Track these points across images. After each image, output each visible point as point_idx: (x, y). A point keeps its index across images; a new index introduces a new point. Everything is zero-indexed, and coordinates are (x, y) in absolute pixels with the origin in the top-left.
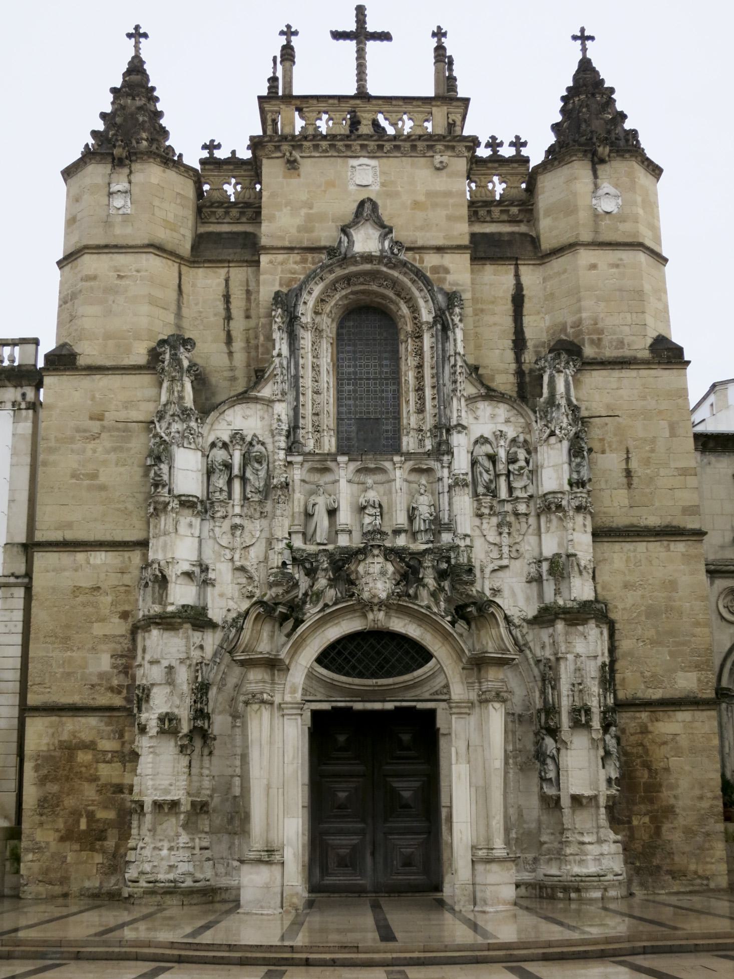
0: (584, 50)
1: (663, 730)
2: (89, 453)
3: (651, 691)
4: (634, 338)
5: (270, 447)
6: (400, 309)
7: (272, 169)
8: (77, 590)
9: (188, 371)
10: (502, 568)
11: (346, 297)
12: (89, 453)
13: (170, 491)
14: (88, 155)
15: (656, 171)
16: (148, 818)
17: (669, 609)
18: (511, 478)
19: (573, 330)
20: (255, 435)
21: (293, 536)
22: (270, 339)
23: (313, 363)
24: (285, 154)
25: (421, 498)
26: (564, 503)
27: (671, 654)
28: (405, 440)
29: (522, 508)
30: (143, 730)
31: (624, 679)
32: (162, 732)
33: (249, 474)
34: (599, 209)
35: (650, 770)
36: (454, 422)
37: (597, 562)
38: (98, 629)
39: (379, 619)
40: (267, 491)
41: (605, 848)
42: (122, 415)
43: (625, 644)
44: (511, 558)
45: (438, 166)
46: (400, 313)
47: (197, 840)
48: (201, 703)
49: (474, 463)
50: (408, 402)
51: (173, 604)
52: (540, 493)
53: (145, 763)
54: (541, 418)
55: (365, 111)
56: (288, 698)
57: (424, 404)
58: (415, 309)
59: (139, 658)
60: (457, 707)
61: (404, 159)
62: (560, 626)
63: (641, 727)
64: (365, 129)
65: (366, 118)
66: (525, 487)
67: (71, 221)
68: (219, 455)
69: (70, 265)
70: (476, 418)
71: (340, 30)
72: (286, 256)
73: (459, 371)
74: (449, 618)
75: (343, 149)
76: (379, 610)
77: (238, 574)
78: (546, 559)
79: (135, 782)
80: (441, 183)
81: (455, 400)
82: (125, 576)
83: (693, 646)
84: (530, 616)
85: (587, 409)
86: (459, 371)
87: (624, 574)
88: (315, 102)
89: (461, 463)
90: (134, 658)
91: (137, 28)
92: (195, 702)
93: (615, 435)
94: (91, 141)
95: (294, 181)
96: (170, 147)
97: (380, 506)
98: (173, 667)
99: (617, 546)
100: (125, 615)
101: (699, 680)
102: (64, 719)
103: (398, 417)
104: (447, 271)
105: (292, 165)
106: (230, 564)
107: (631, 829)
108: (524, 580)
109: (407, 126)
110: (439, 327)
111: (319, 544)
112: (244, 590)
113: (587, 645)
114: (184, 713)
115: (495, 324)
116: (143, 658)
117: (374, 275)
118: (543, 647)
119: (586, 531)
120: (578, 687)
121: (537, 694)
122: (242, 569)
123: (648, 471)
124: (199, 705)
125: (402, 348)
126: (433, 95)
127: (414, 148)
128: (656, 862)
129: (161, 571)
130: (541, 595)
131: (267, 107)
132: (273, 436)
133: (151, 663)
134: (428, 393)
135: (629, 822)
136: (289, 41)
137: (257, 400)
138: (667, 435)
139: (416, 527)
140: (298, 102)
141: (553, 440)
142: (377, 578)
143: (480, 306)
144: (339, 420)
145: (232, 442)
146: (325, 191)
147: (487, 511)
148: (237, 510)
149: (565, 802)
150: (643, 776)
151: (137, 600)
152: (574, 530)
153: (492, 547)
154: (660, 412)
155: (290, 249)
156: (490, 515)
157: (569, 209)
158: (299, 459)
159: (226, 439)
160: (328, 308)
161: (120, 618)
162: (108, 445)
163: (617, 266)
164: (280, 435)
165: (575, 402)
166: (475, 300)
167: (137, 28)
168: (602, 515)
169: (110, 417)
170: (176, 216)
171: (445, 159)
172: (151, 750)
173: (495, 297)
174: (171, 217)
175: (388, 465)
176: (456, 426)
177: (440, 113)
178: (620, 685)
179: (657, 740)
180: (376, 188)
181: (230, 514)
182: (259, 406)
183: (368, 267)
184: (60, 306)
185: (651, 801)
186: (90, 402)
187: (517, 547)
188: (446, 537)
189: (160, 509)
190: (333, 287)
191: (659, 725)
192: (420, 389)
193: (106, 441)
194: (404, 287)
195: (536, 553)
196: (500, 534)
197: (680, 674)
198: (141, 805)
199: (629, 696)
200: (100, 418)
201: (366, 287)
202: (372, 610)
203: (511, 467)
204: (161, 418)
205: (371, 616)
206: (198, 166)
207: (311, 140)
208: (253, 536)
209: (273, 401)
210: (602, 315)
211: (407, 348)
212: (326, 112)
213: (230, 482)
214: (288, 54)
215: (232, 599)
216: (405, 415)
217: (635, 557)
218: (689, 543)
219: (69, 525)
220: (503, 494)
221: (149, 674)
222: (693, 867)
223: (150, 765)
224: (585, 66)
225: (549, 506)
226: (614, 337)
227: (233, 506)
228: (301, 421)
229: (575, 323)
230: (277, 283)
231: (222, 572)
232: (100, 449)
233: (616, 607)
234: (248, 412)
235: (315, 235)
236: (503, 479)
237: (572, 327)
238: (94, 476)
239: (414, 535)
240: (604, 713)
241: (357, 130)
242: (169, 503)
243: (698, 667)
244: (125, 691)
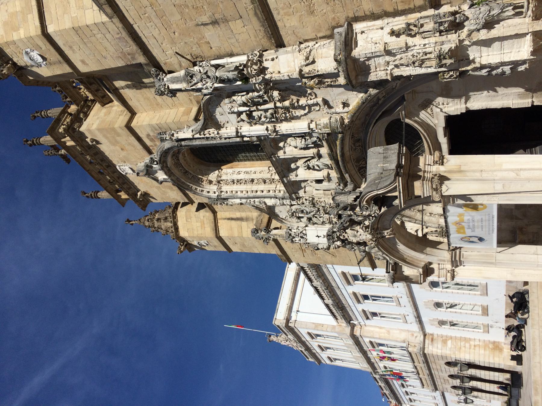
10: (326, 102)
43: (367, 7)
70: (228, 122)
73: (203, 136)
75: (121, 179)
99: (279, 24)
119: (277, 58)
152: (279, 72)
168: (258, 39)
170: (197, 222)
173: (145, 99)
174: (199, 224)
217: (283, 9)
228: (272, 194)
233: (334, 18)
240: (441, 32)
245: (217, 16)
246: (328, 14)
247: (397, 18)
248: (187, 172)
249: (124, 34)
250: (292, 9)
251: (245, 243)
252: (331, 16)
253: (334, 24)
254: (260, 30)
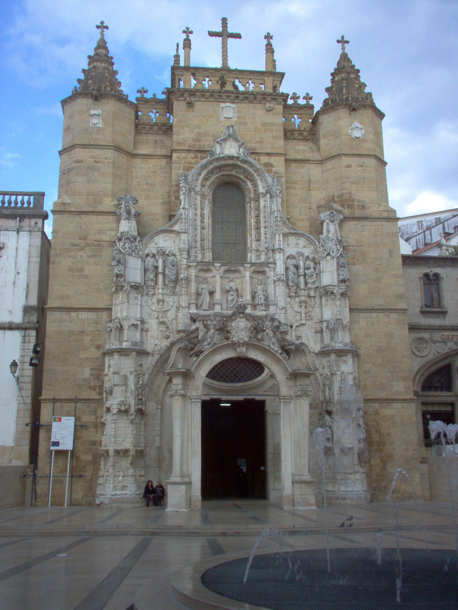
0: (343, 48)
2: (79, 258)
4: (371, 204)
5: (178, 257)
6: (247, 185)
7: (179, 106)
8: (71, 332)
9: (134, 215)
11: (218, 178)
12: (79, 258)
13: (125, 279)
14: (76, 95)
15: (381, 116)
16: (111, 459)
18: (307, 277)
19: (338, 199)
20: (170, 251)
21: (191, 306)
22: (178, 198)
23: (201, 213)
24: (186, 99)
25: (259, 286)
26: (335, 291)
28: (249, 255)
29: (312, 293)
30: (108, 410)
32: (120, 411)
33: (166, 272)
34: (353, 135)
35: (379, 433)
36: (276, 247)
37: (352, 322)
38: (83, 355)
39: (242, 351)
40: (176, 281)
41: (358, 476)
42: (97, 237)
44: (306, 320)
45: (268, 109)
46: (247, 187)
47: (138, 472)
48: (141, 395)
49: (287, 269)
50: (251, 235)
51: (126, 341)
52: (322, 285)
53: (109, 429)
54: (323, 246)
55: (229, 77)
56: (194, 393)
57: (260, 236)
58: (255, 186)
59: (106, 371)
60: (284, 399)
61: (250, 104)
62: (333, 357)
64: (229, 87)
65: (229, 80)
66: (314, 282)
67: (67, 129)
68: (150, 261)
69: (67, 153)
70: (288, 245)
71: (214, 30)
72: (186, 154)
75: (217, 97)
76: (243, 346)
77: (161, 325)
78: (325, 321)
79: (103, 439)
80: (269, 118)
81: (277, 235)
82: (98, 325)
84: (316, 351)
85: (346, 242)
86: (279, 220)
88: (202, 71)
89: (280, 268)
90: (103, 370)
91: (102, 23)
92: (138, 395)
94: (78, 86)
95: (191, 114)
96: (121, 90)
97: (237, 290)
98: (126, 376)
100: (98, 347)
101: (405, 387)
102: (63, 404)
103: (245, 244)
104: (272, 166)
105: (190, 105)
106: (157, 320)
107: (370, 466)
108: (313, 331)
109: (251, 87)
110: (268, 195)
111: (205, 310)
112: (164, 334)
113: (347, 366)
114: (132, 401)
115: (296, 195)
116: (109, 371)
117: (235, 166)
118: (324, 368)
121: (321, 393)
122: (163, 323)
123: (378, 275)
124: (140, 397)
125: (248, 206)
126: (264, 70)
127: (255, 98)
128: (384, 484)
129: (120, 323)
130: (322, 340)
131: (176, 72)
132: (180, 251)
133: (115, 373)
134: (262, 230)
135: (369, 462)
136: (188, 37)
137: (172, 232)
138: (387, 256)
139: (256, 302)
140: (193, 71)
141: (329, 258)
142: (240, 329)
143: (288, 185)
144: (214, 243)
145: (158, 254)
146: (207, 120)
147: (293, 295)
148: (160, 291)
149: (337, 451)
150: (376, 437)
151: (105, 339)
153: (297, 314)
155: (189, 151)
156: (295, 296)
157: (337, 135)
158: (195, 264)
159: (155, 252)
160: (208, 183)
161: (95, 348)
162: (89, 253)
163: (362, 166)
164: (184, 251)
165: (340, 238)
166: (287, 182)
167: (102, 23)
169: (92, 237)
171: (271, 105)
172: (114, 421)
175: (241, 268)
176: (278, 249)
177: (269, 81)
180: (235, 119)
181: (157, 293)
182: (172, 235)
183: (231, 162)
184: (60, 176)
185: (381, 451)
186: (79, 230)
188: (272, 309)
189: (119, 288)
190: (212, 172)
192: (258, 228)
193: (88, 251)
194: (249, 173)
195: (319, 317)
196: (301, 307)
197: (395, 382)
198: (107, 452)
200: (85, 238)
201: (229, 173)
202: (239, 346)
203: (306, 271)
204: (120, 240)
205: (238, 350)
206: (136, 102)
207: (201, 92)
208: (169, 305)
209: (180, 233)
210: (353, 192)
211: (250, 207)
212: (208, 77)
213: (156, 276)
214: (187, 44)
215: (157, 339)
216: (249, 242)
218: (400, 314)
219: (67, 297)
220: (302, 286)
221: (110, 380)
222: (403, 487)
223: (113, 430)
224: (344, 57)
225: (327, 292)
226: (360, 204)
227: (158, 288)
229: (339, 196)
230: (182, 169)
231: (153, 324)
232: (85, 256)
233: (361, 347)
234: (167, 238)
235: (202, 143)
236: (302, 278)
237: (337, 198)
238: (82, 270)
239: (254, 307)
241: (225, 87)
242: (124, 286)
244: (98, 389)
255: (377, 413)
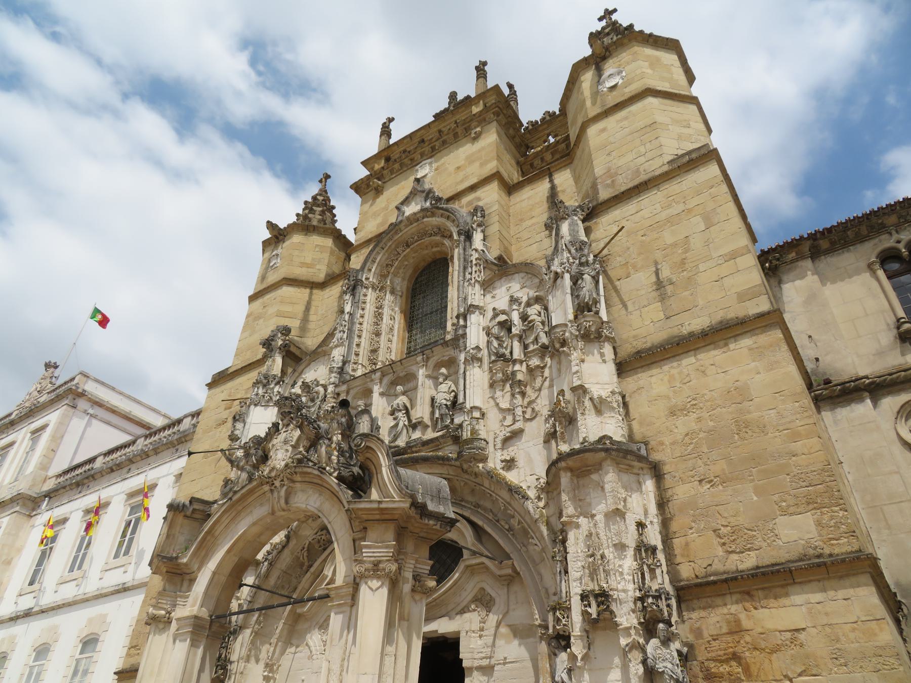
1: (770, 625)
3: (735, 557)
17: (743, 426)
27: (758, 491)
29: (535, 362)
31: (687, 544)
43: (681, 492)
63: (728, 622)
74: (335, 474)
83: (796, 471)
87: (668, 398)
93: (640, 254)
101: (819, 524)
120: (596, 565)
154: (690, 211)
170: (313, 259)
174: (308, 260)
178: (682, 556)
179: (763, 645)
187: (534, 405)
191: (762, 613)
197: (781, 520)
199: (701, 572)
217: (680, 373)
220: (518, 353)
228: (353, 357)
233: (662, 444)
240: (642, 599)
243: (811, 503)
245: (669, 289)
246: (668, 440)
247: (659, 537)
248: (408, 246)
249: (643, 177)
250: (678, 385)
251: (261, 321)
252: (667, 440)
253: (653, 443)
254: (645, 343)
255: (736, 629)
